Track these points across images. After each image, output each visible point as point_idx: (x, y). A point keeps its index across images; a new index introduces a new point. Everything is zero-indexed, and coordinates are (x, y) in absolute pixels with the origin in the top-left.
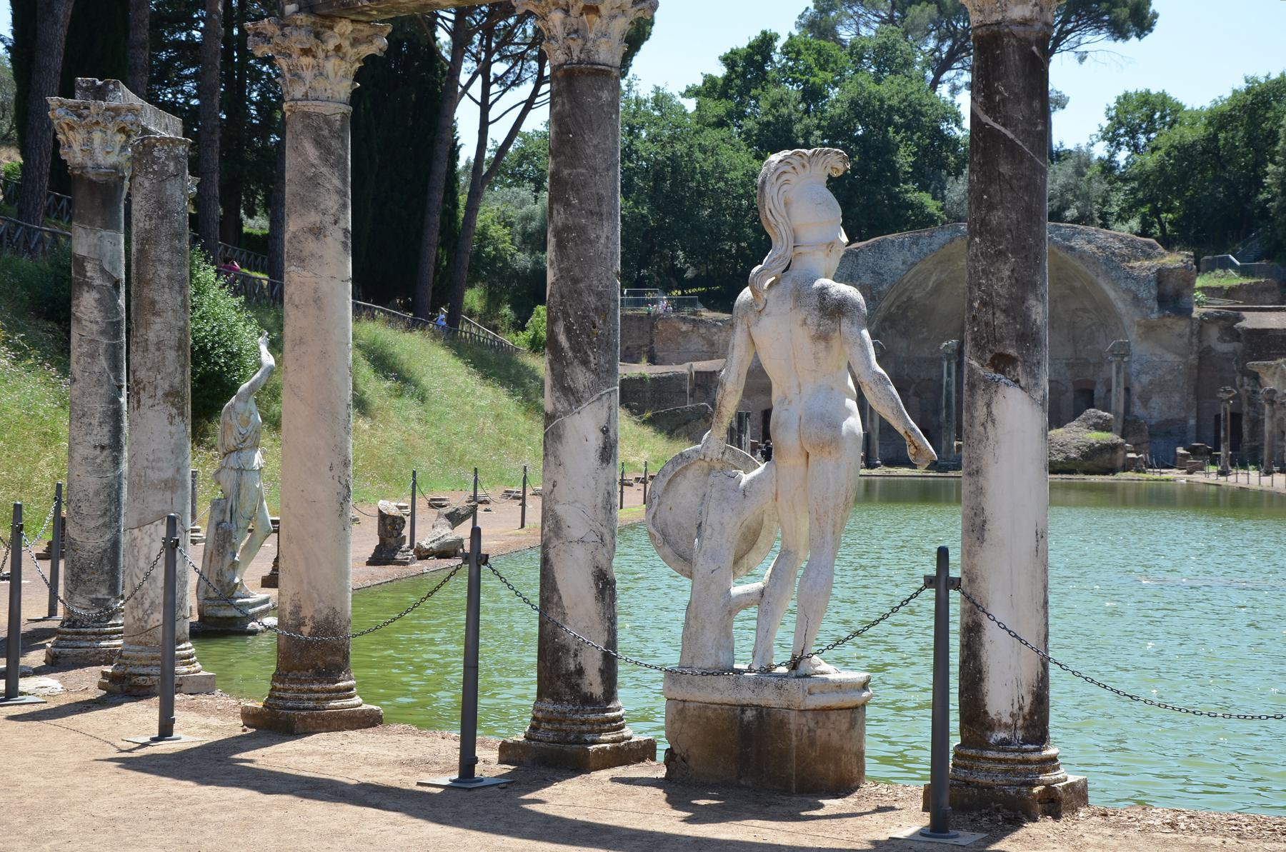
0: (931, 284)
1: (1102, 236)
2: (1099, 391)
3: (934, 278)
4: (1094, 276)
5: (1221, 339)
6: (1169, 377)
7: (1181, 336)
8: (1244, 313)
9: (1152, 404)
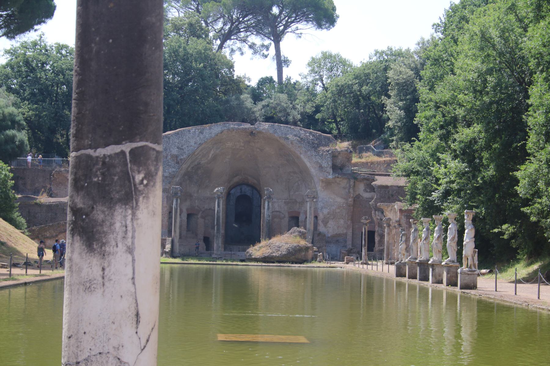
0: (211, 155)
2: (301, 218)
3: (212, 152)
4: (298, 153)
5: (365, 191)
6: (338, 211)
7: (344, 188)
8: (376, 177)
9: (329, 225)
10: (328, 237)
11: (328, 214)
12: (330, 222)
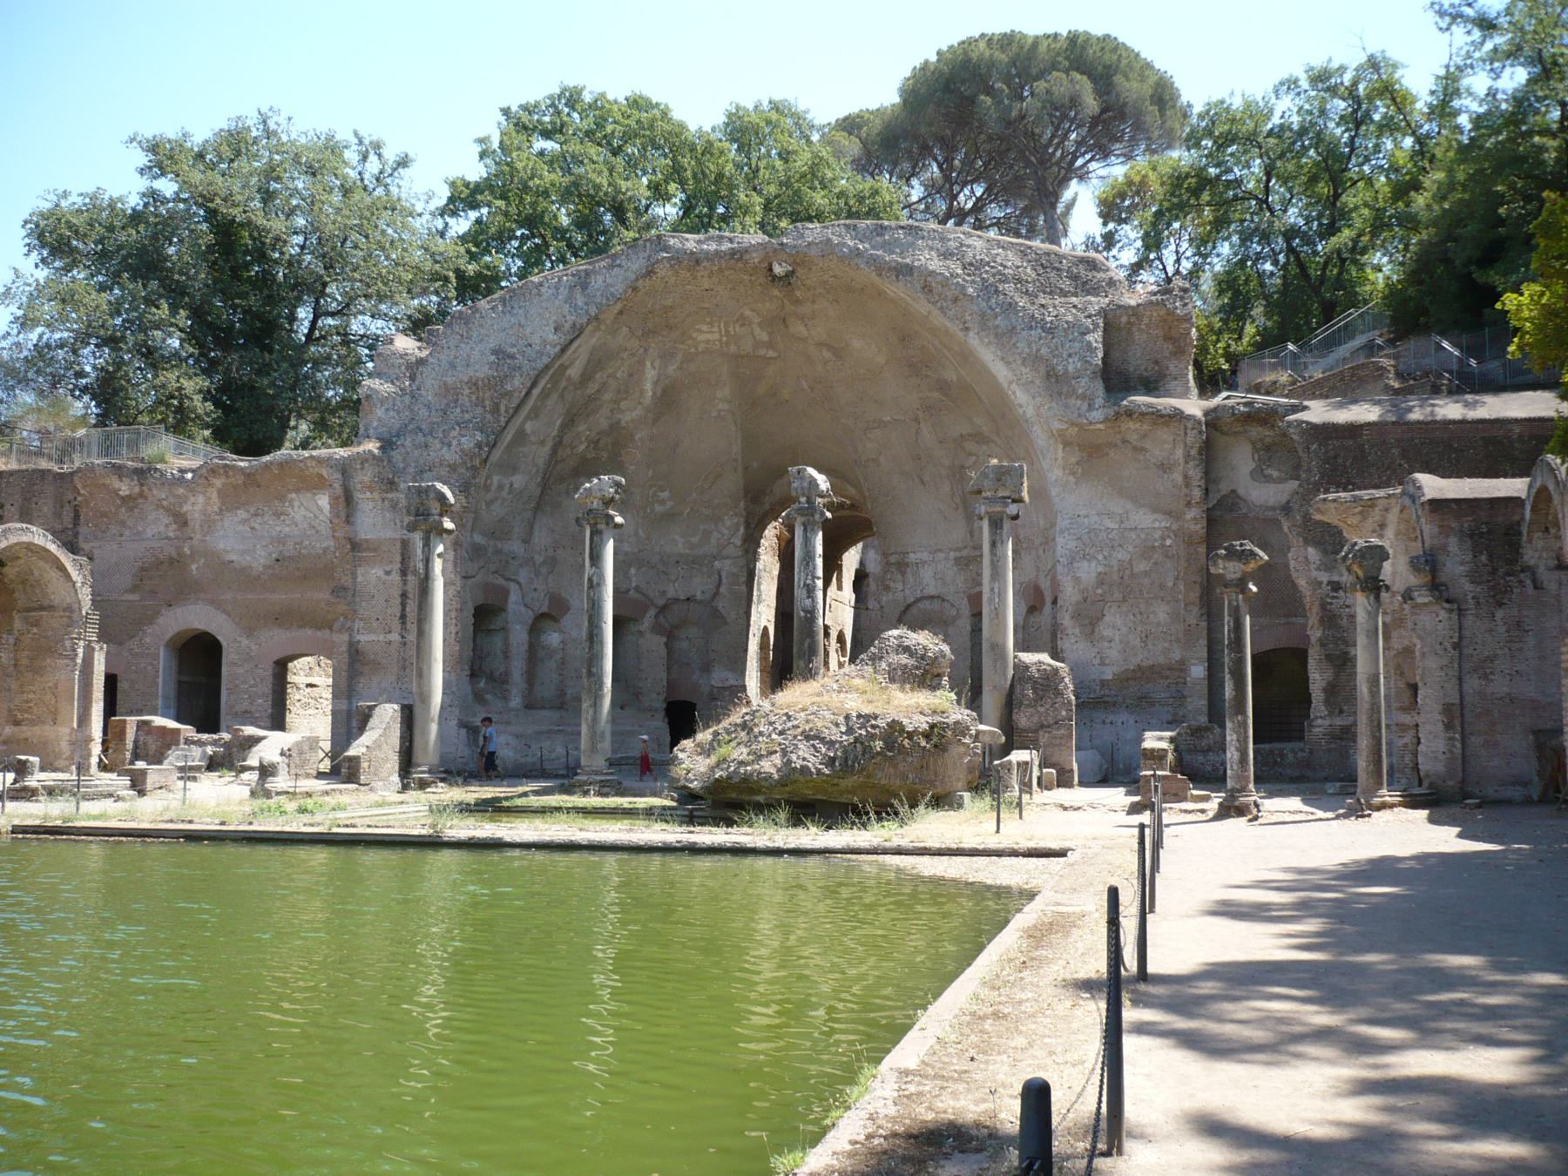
0: (648, 386)
1: (978, 244)
3: (650, 374)
4: (954, 328)
5: (1259, 475)
6: (1142, 566)
7: (1165, 467)
10: (1103, 683)
11: (1101, 583)
12: (1107, 618)
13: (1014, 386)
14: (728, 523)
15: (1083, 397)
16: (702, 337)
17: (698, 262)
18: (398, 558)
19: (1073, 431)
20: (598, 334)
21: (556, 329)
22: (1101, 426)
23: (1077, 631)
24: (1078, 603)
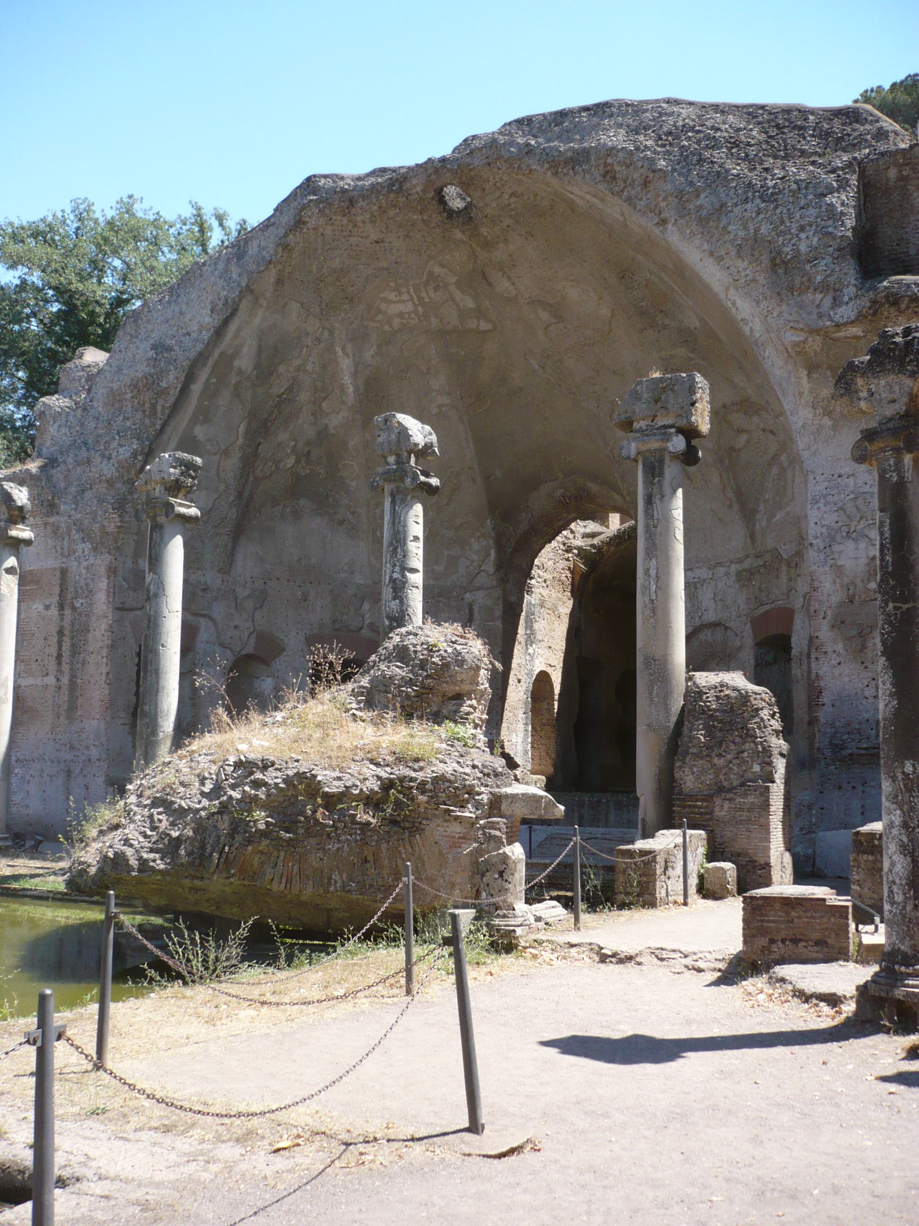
0: (347, 379)
3: (346, 364)
13: (732, 291)
14: (476, 546)
15: (824, 287)
16: (395, 309)
17: (352, 202)
18: (57, 590)
19: (815, 343)
20: (260, 312)
21: (212, 311)
22: (856, 330)
23: (840, 647)
24: (841, 605)
